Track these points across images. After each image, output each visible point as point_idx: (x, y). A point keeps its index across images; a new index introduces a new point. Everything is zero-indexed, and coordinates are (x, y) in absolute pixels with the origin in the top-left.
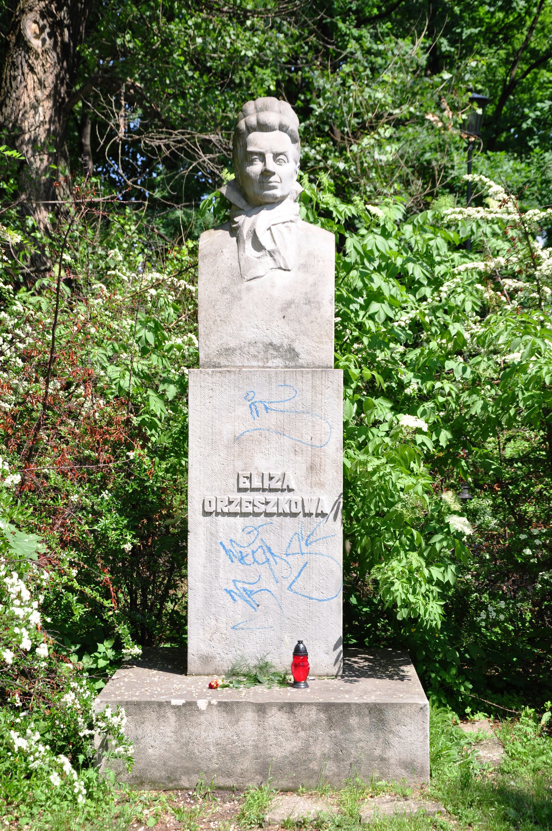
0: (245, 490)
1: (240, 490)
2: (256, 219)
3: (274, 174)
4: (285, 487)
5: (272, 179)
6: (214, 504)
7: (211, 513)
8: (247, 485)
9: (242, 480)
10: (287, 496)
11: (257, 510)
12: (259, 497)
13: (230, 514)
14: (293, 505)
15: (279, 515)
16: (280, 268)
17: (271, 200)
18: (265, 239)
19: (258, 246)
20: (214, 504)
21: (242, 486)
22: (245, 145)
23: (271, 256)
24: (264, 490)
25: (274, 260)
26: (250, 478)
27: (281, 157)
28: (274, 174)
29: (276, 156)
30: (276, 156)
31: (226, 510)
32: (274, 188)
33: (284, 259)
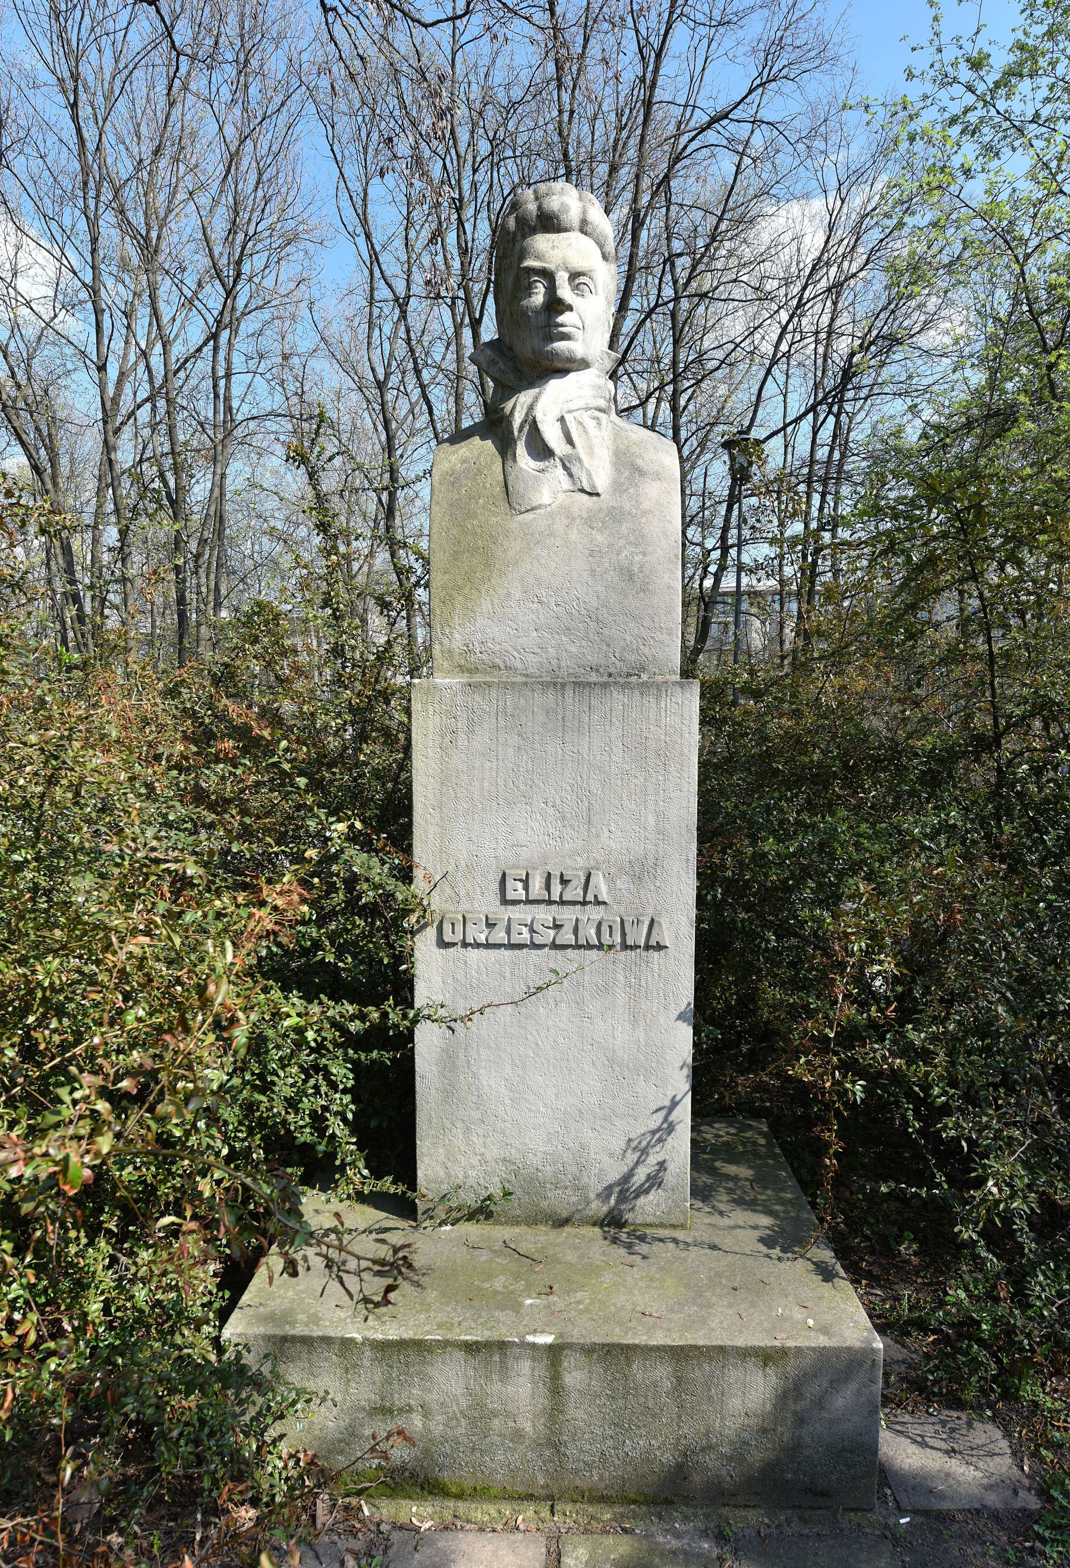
0: (515, 902)
1: (505, 902)
2: (536, 399)
3: (570, 308)
4: (590, 897)
5: (564, 318)
6: (459, 928)
7: (454, 944)
8: (521, 894)
9: (510, 884)
10: (595, 913)
11: (538, 940)
12: (544, 915)
13: (488, 946)
14: (605, 929)
15: (578, 947)
16: (582, 491)
17: (559, 365)
18: (552, 435)
19: (541, 450)
20: (459, 928)
21: (510, 895)
22: (523, 255)
23: (565, 467)
24: (550, 902)
25: (571, 475)
26: (526, 883)
27: (582, 279)
28: (570, 308)
29: (574, 275)
30: (574, 275)
31: (482, 938)
32: (566, 337)
33: (589, 475)
